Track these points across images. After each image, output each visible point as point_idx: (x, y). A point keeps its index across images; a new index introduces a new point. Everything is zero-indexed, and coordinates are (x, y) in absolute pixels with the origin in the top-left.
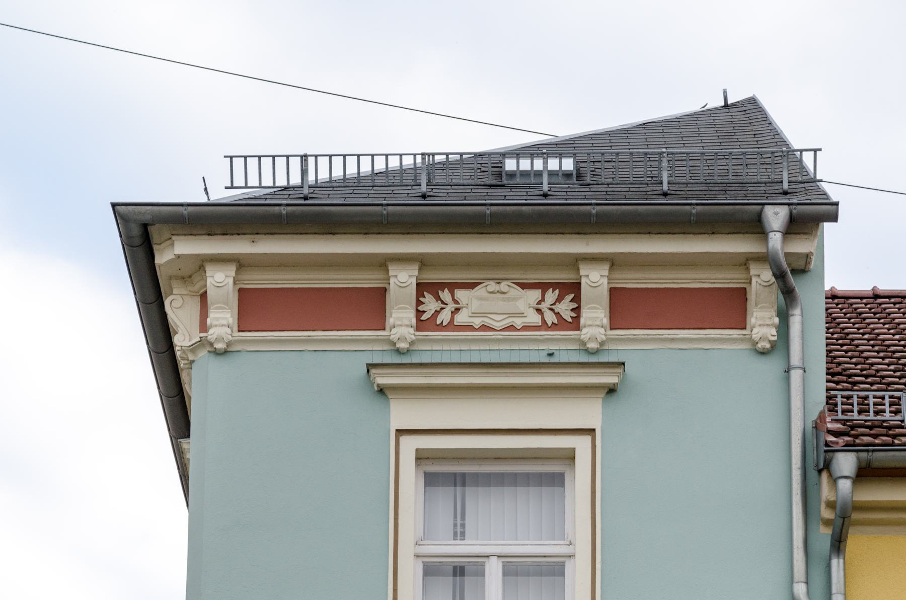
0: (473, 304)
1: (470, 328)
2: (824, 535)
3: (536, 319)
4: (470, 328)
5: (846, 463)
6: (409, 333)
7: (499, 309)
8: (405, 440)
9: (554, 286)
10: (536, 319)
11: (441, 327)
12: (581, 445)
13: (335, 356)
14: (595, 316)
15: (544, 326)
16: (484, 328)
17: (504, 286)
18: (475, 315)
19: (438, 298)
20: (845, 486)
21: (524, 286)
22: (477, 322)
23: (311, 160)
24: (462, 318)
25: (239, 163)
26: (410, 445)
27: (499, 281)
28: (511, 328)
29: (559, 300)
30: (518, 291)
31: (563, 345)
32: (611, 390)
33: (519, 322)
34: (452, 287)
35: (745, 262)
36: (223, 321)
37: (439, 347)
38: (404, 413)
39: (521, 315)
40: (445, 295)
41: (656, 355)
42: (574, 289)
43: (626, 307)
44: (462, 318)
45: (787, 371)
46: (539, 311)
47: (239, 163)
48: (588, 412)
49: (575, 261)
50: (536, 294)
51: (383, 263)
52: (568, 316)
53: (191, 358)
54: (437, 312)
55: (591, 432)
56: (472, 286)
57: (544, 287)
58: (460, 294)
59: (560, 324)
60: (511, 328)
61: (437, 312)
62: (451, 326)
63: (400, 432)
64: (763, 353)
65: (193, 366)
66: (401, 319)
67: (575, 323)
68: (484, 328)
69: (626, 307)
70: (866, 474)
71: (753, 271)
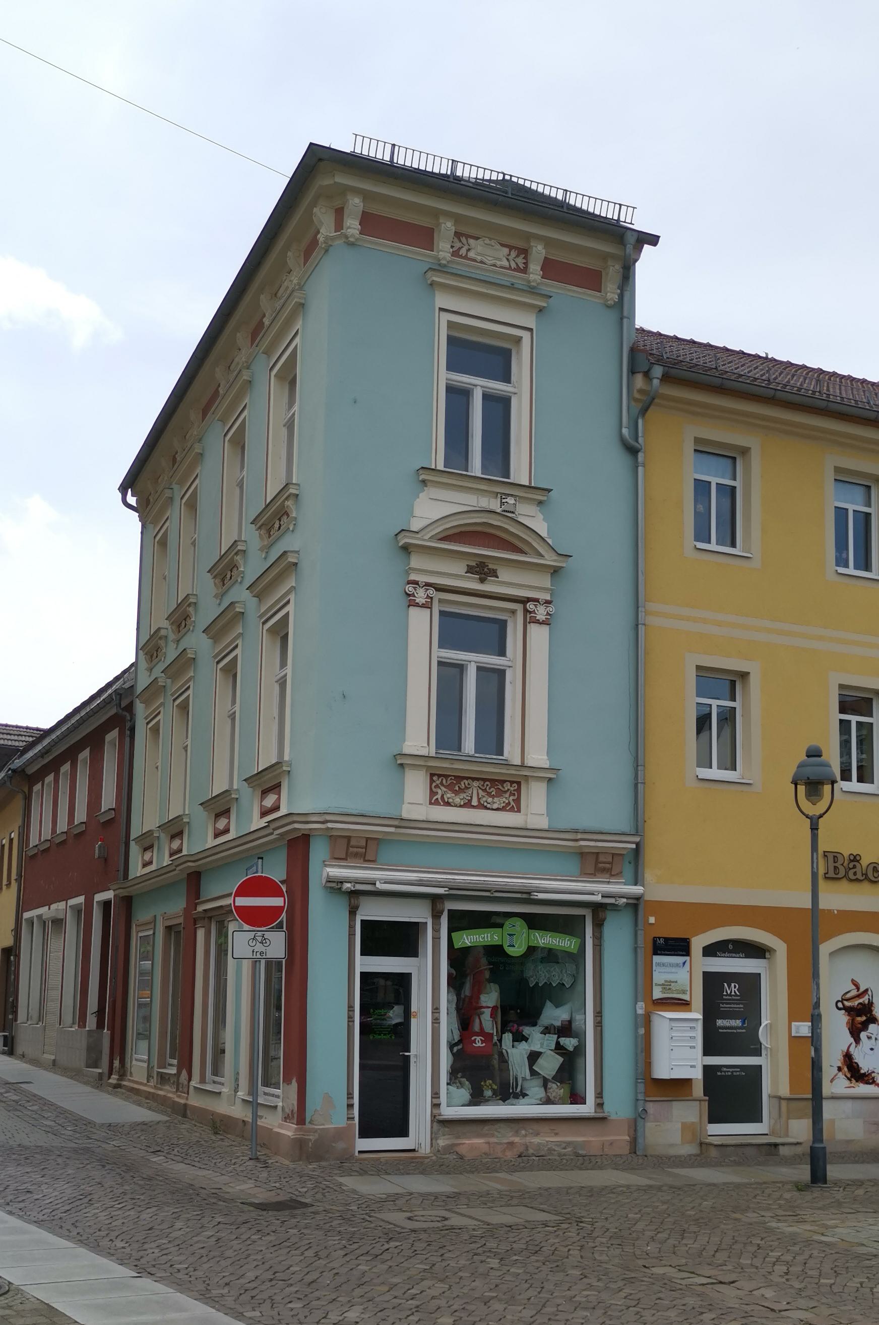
0: (478, 249)
1: (475, 260)
2: (636, 407)
3: (506, 263)
4: (475, 260)
5: (658, 371)
6: (448, 256)
7: (489, 254)
8: (443, 314)
9: (516, 248)
10: (506, 263)
11: (461, 257)
12: (526, 335)
13: (408, 260)
14: (535, 268)
15: (510, 268)
16: (482, 262)
17: (492, 242)
18: (479, 254)
19: (460, 241)
20: (656, 382)
21: (502, 245)
22: (479, 258)
23: (397, 148)
24: (471, 254)
25: (359, 139)
26: (445, 317)
27: (490, 239)
28: (494, 265)
29: (517, 256)
30: (498, 247)
31: (518, 279)
32: (541, 310)
33: (498, 263)
34: (468, 236)
35: (605, 257)
36: (352, 225)
37: (460, 266)
38: (442, 300)
39: (500, 260)
40: (464, 239)
41: (565, 296)
42: (524, 252)
43: (551, 269)
44: (471, 254)
45: (622, 319)
46: (508, 259)
47: (359, 139)
48: (529, 320)
49: (529, 237)
50: (506, 250)
51: (436, 214)
52: (521, 266)
53: (330, 243)
54: (460, 248)
55: (531, 330)
56: (477, 238)
57: (511, 248)
58: (471, 241)
59: (518, 269)
60: (494, 265)
61: (460, 248)
62: (466, 257)
63: (441, 309)
64: (608, 307)
65: (331, 249)
66: (443, 248)
67: (525, 270)
68: (482, 262)
69: (551, 269)
70: (666, 378)
71: (610, 263)
